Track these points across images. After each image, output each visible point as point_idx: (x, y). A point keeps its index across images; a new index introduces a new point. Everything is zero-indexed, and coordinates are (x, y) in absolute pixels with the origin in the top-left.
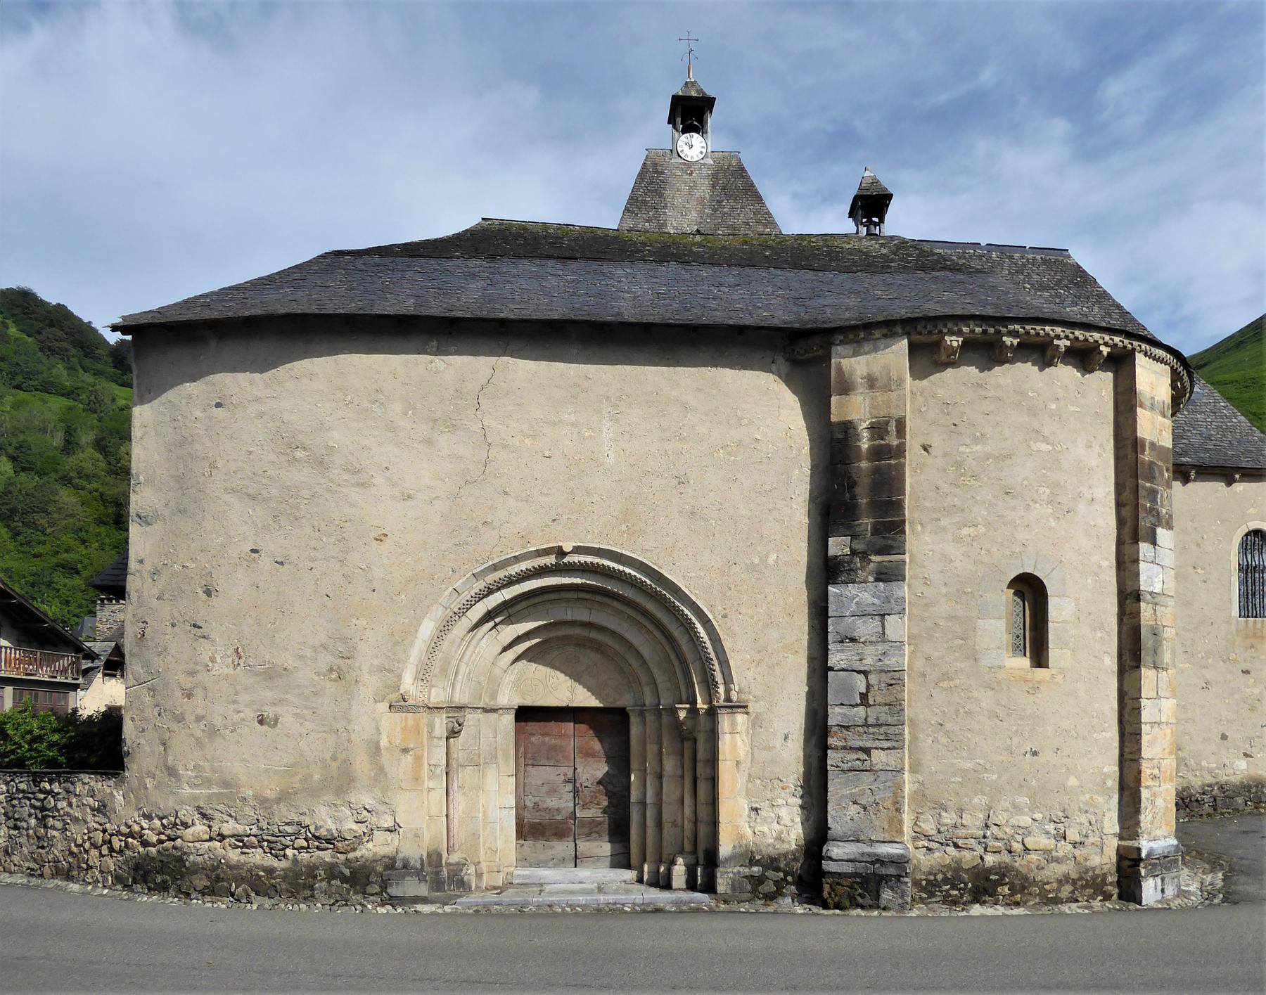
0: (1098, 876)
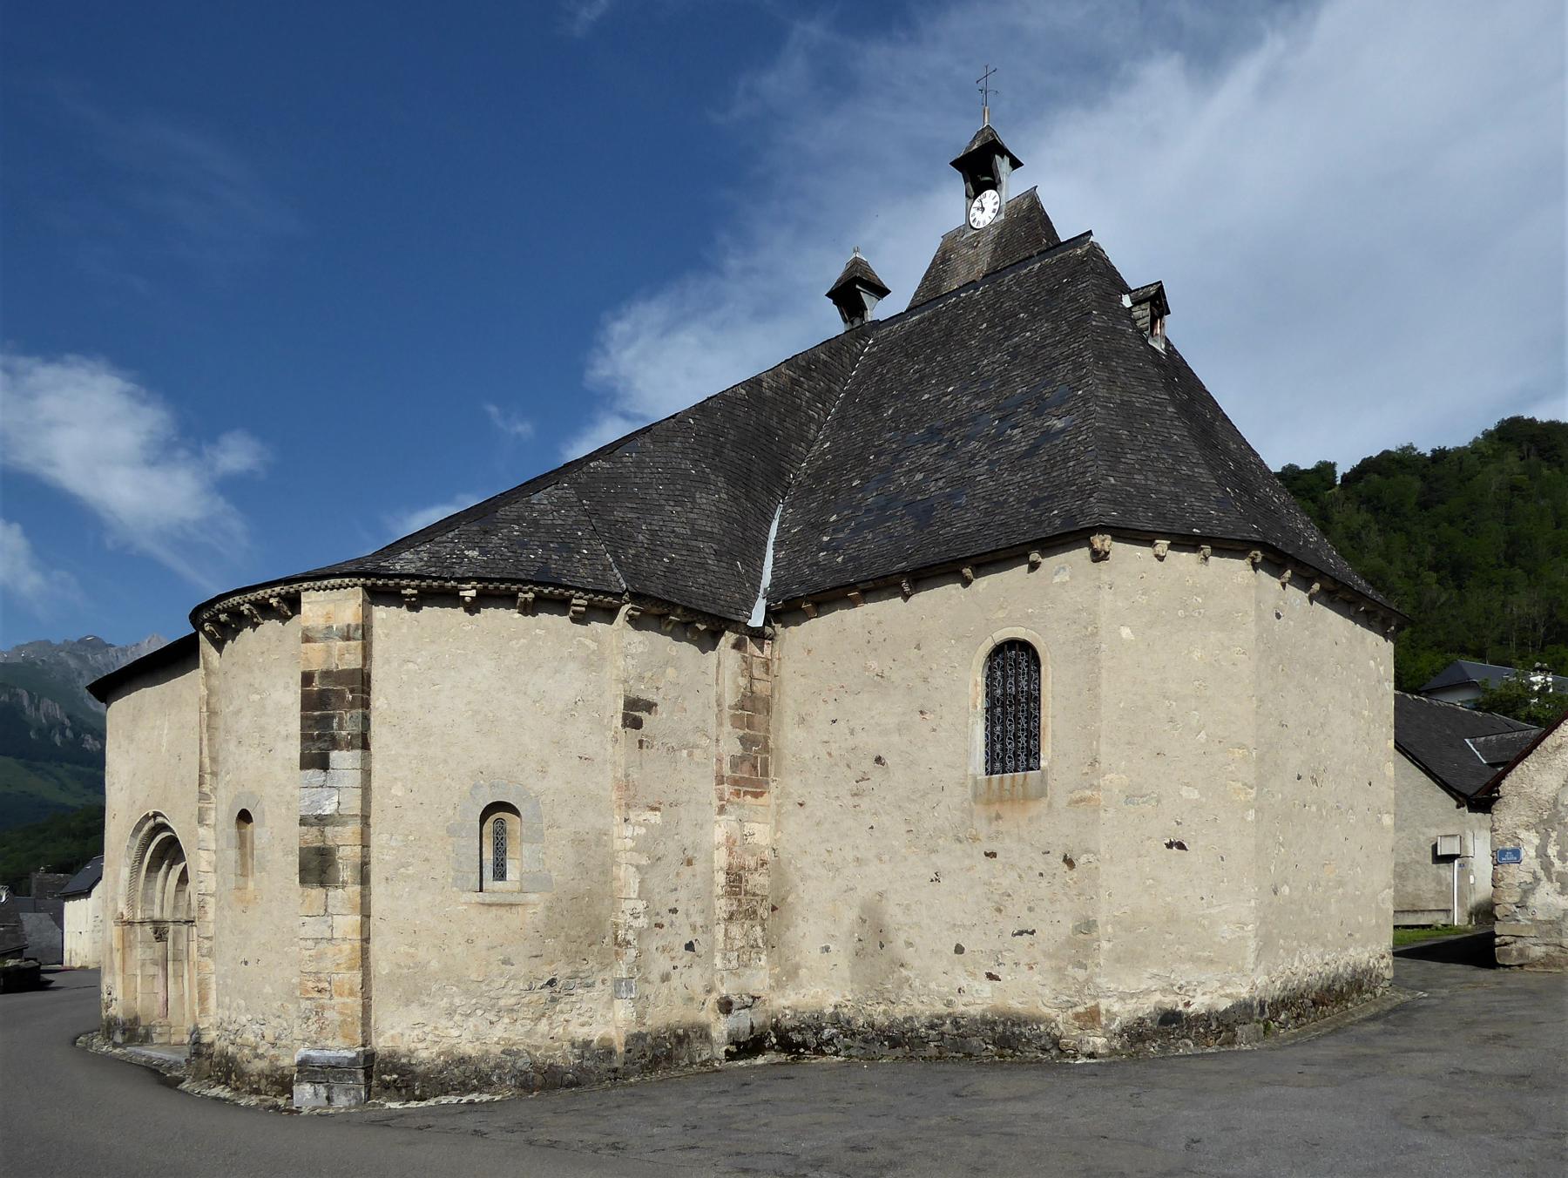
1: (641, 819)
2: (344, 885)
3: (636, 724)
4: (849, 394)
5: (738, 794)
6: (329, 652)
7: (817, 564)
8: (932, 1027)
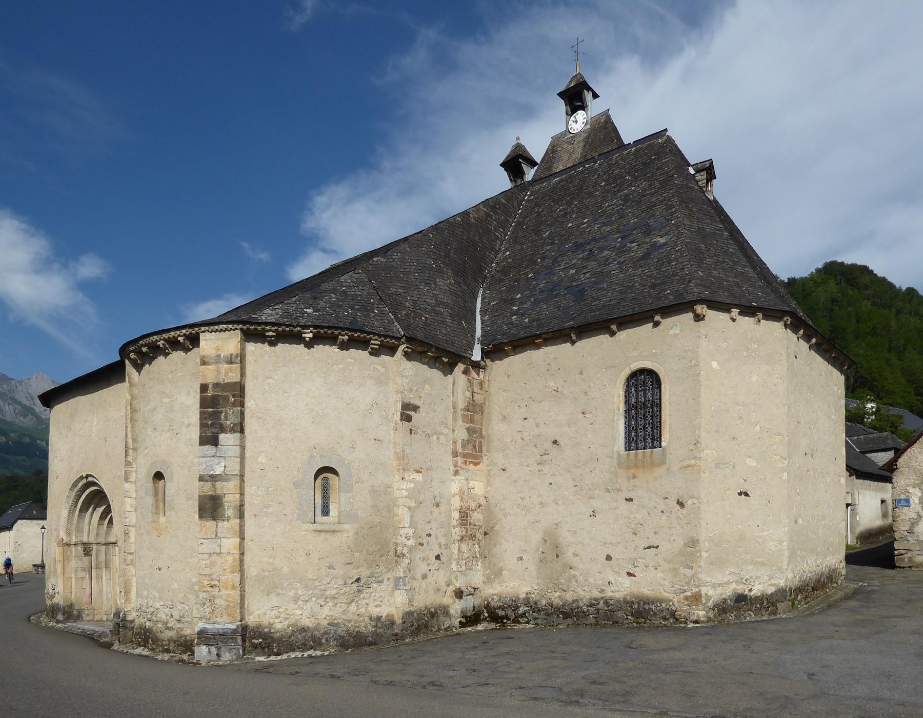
0: (188, 641)
1: (411, 478)
2: (228, 519)
3: (408, 419)
4: (518, 223)
5: (465, 463)
6: (218, 372)
7: (512, 323)
8: (591, 605)
